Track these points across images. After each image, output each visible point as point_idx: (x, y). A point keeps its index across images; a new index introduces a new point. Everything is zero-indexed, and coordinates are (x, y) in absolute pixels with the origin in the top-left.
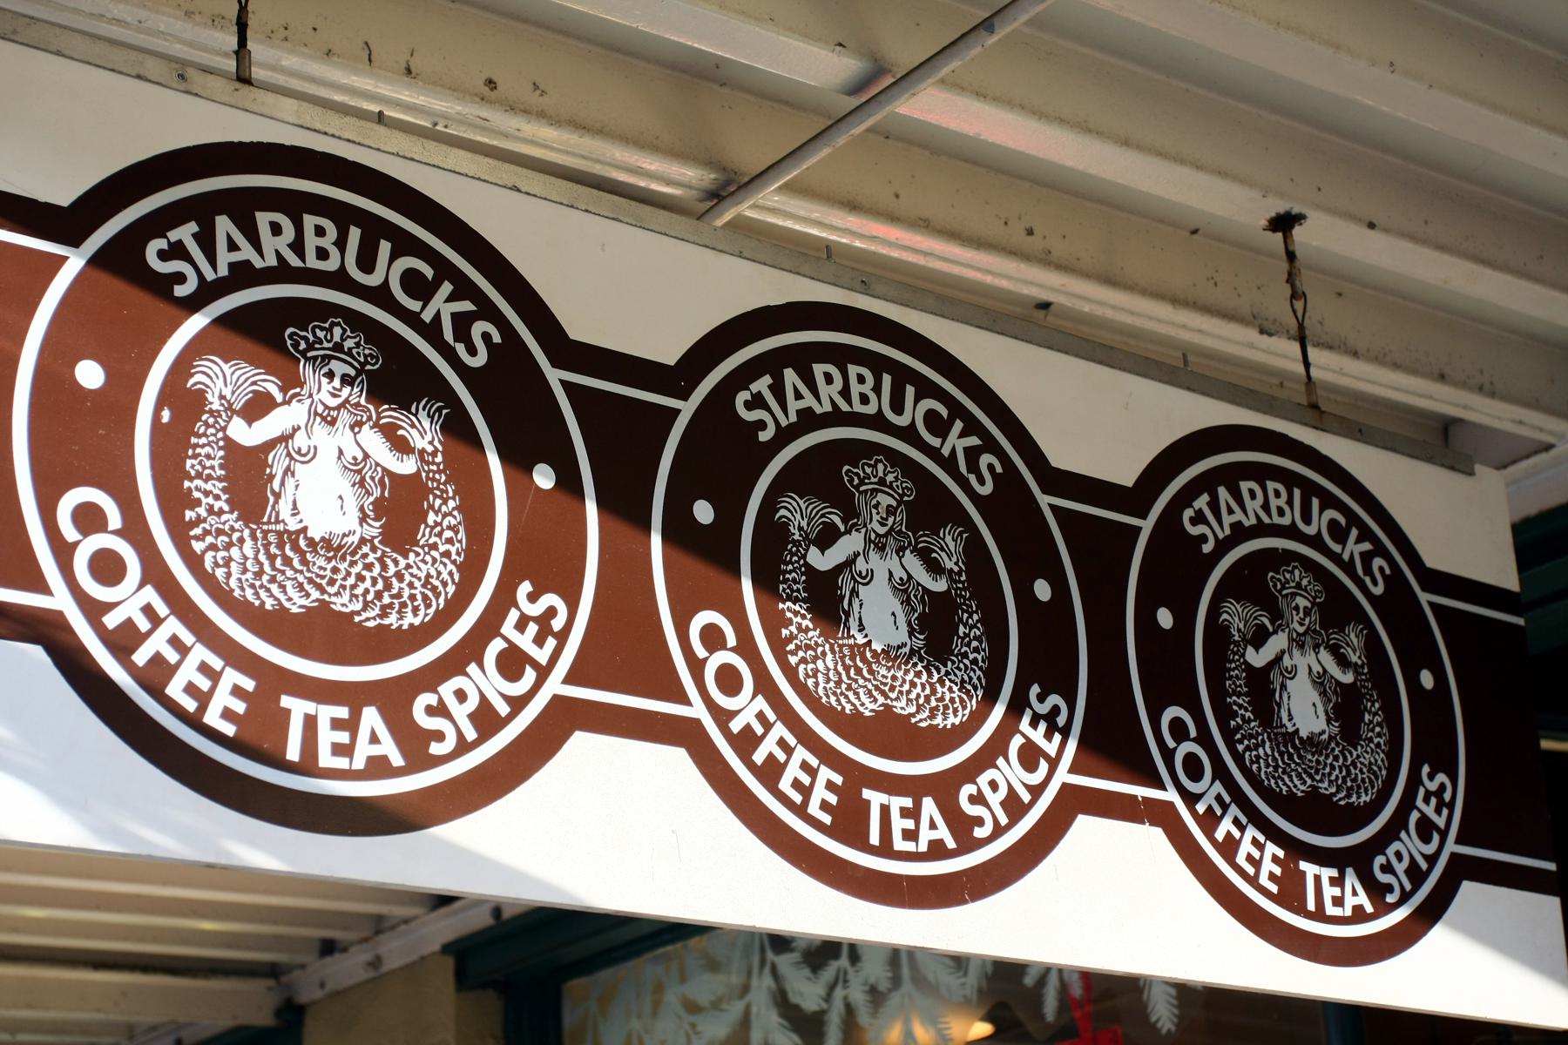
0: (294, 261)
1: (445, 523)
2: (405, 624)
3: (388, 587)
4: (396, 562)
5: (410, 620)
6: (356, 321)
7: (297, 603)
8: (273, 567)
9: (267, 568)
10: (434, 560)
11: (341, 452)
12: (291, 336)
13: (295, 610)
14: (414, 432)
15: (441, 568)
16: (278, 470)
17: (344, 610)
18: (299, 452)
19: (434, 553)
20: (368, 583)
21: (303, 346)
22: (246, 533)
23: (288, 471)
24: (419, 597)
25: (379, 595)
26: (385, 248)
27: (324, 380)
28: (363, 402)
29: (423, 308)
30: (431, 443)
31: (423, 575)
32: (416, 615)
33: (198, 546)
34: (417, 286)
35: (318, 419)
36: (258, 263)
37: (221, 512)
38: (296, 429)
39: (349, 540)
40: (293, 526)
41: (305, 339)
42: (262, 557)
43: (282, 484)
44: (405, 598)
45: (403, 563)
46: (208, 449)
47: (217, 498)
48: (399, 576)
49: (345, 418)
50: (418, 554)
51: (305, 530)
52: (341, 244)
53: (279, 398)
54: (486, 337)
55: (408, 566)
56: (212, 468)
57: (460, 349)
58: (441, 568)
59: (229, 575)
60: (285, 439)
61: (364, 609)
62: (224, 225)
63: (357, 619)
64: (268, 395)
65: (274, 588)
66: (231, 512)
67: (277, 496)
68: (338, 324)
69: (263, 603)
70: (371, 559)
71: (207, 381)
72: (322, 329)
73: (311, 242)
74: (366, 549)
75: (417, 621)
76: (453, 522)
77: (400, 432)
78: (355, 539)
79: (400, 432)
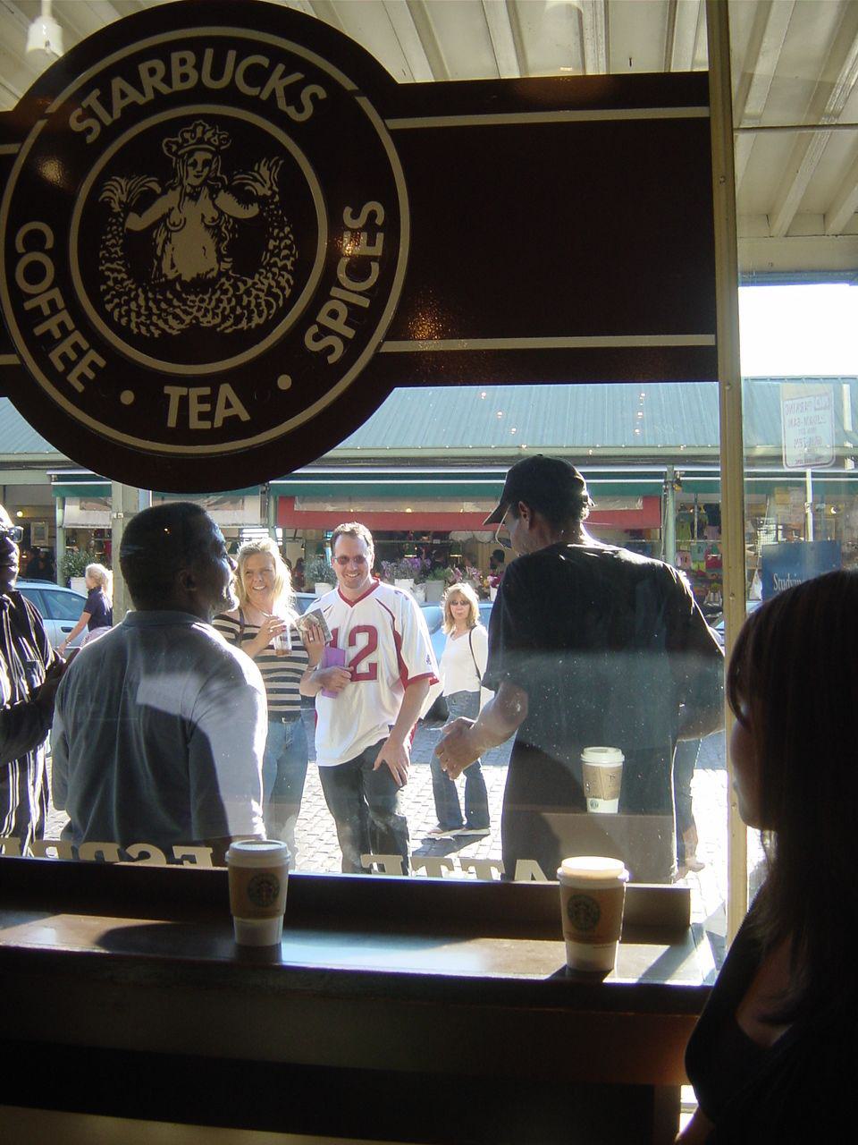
0: (165, 89)
1: (282, 245)
2: (253, 325)
3: (239, 299)
4: (245, 283)
5: (257, 320)
6: (212, 120)
7: (175, 328)
8: (159, 308)
9: (155, 311)
10: (274, 274)
11: (203, 217)
12: (167, 145)
13: (175, 333)
14: (257, 185)
15: (280, 279)
16: (160, 240)
17: (209, 325)
18: (174, 225)
19: (275, 270)
20: (225, 304)
21: (174, 148)
22: (140, 290)
23: (168, 240)
24: (263, 303)
25: (233, 310)
26: (232, 55)
27: (190, 169)
28: (219, 174)
29: (260, 93)
30: (270, 189)
31: (265, 288)
32: (260, 316)
33: (109, 307)
34: (257, 76)
35: (187, 198)
36: (141, 101)
37: (123, 280)
38: (171, 210)
39: (210, 276)
40: (171, 275)
41: (176, 143)
42: (151, 304)
43: (163, 251)
44: (253, 306)
45: (250, 282)
46: (113, 241)
47: (119, 272)
48: (248, 292)
49: (205, 191)
50: (261, 274)
51: (180, 275)
52: (198, 67)
53: (159, 190)
54: (314, 97)
55: (255, 284)
56: (116, 253)
57: (291, 111)
58: (280, 279)
59: (129, 321)
60: (166, 216)
61: (223, 321)
62: (118, 84)
63: (218, 329)
64: (151, 189)
65: (161, 323)
66: (129, 279)
67: (160, 259)
68: (200, 124)
69: (152, 334)
70: (227, 285)
71: (112, 195)
72: (188, 131)
73: (177, 71)
74: (223, 280)
75: (261, 321)
76: (288, 242)
77: (247, 188)
78: (214, 274)
79: (247, 188)
